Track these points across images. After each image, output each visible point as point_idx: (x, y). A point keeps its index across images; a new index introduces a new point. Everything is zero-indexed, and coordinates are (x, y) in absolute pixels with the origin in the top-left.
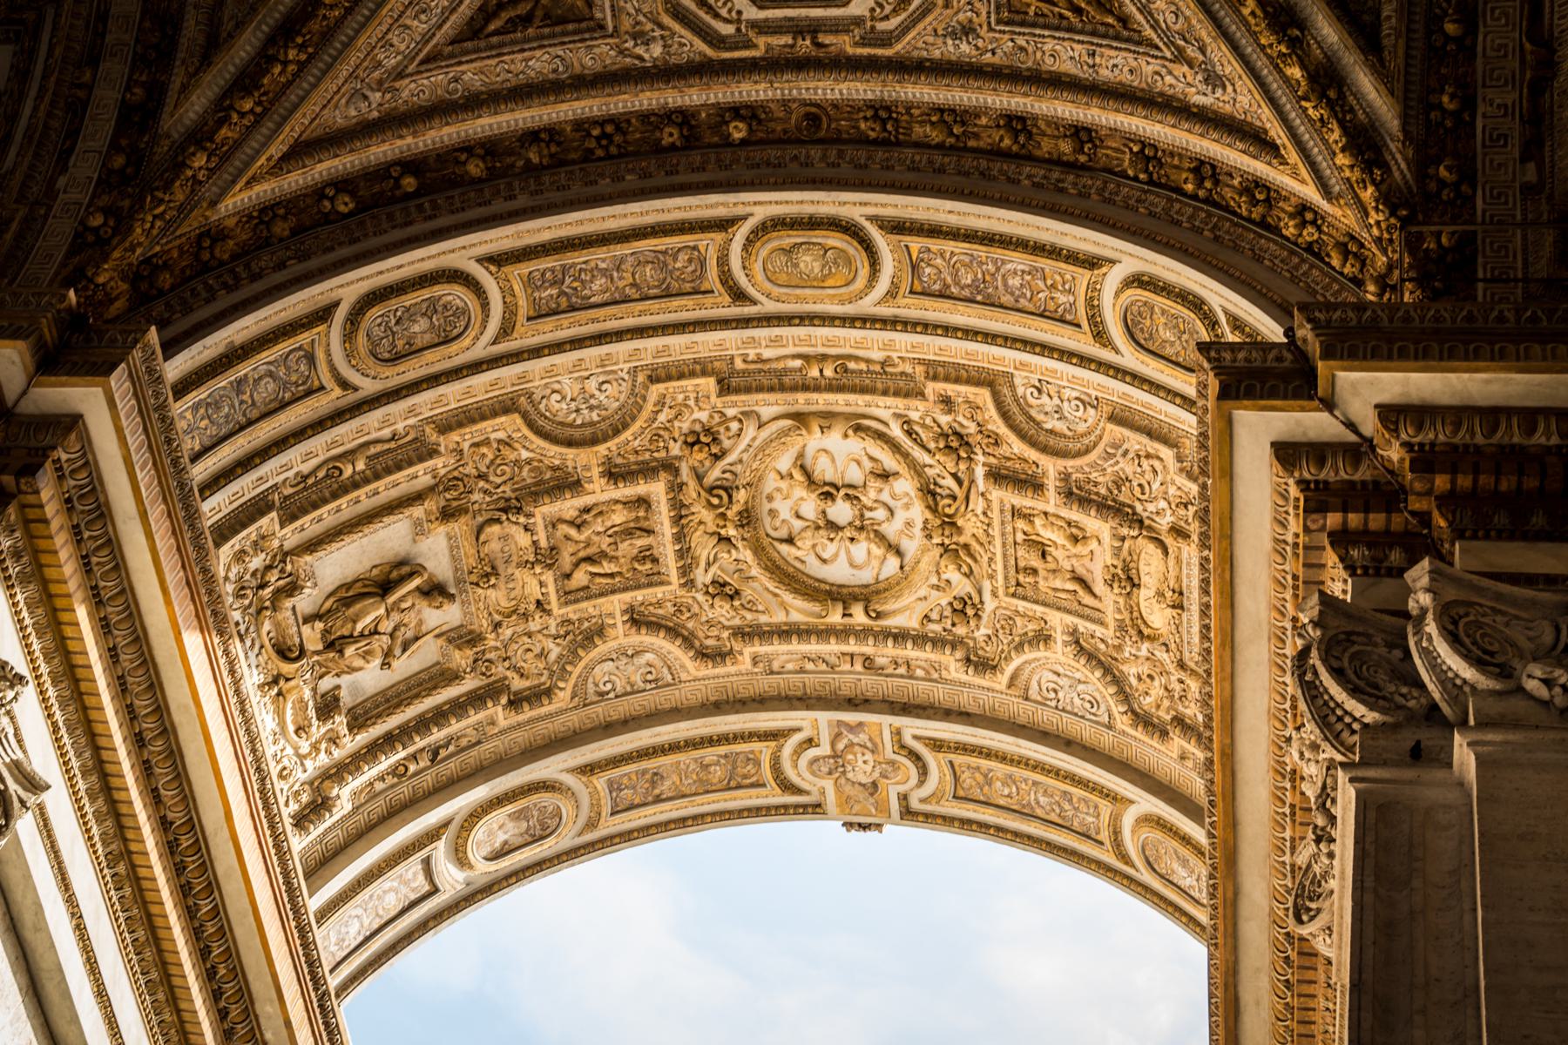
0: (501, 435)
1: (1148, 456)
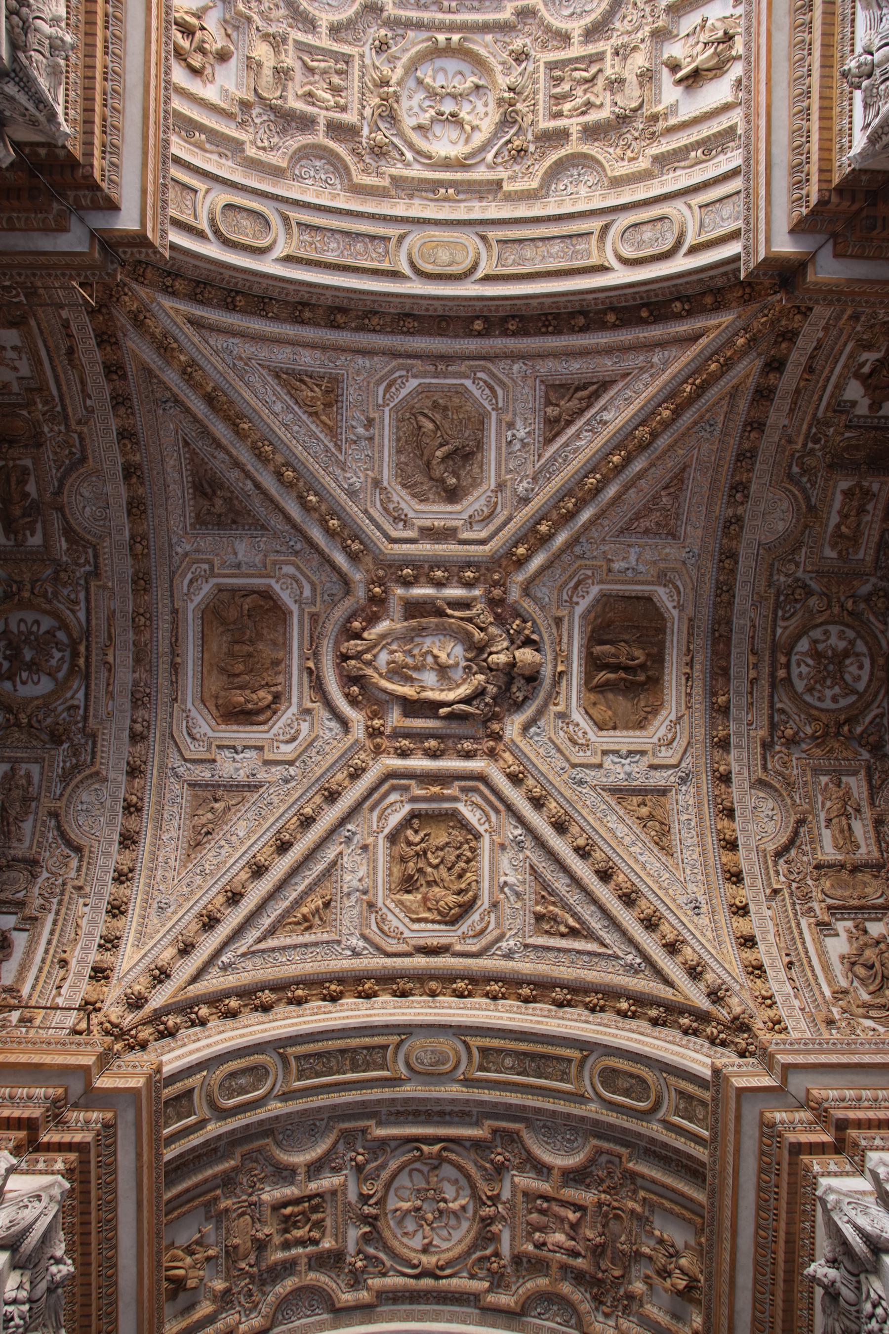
0: (621, 164)
1: (264, 149)
